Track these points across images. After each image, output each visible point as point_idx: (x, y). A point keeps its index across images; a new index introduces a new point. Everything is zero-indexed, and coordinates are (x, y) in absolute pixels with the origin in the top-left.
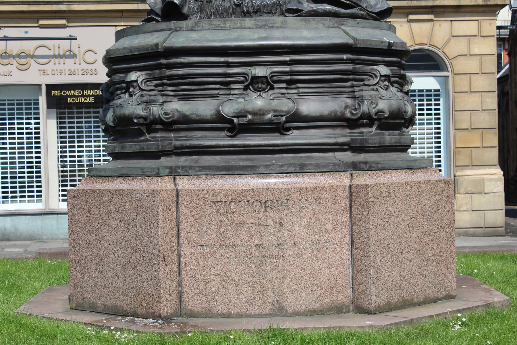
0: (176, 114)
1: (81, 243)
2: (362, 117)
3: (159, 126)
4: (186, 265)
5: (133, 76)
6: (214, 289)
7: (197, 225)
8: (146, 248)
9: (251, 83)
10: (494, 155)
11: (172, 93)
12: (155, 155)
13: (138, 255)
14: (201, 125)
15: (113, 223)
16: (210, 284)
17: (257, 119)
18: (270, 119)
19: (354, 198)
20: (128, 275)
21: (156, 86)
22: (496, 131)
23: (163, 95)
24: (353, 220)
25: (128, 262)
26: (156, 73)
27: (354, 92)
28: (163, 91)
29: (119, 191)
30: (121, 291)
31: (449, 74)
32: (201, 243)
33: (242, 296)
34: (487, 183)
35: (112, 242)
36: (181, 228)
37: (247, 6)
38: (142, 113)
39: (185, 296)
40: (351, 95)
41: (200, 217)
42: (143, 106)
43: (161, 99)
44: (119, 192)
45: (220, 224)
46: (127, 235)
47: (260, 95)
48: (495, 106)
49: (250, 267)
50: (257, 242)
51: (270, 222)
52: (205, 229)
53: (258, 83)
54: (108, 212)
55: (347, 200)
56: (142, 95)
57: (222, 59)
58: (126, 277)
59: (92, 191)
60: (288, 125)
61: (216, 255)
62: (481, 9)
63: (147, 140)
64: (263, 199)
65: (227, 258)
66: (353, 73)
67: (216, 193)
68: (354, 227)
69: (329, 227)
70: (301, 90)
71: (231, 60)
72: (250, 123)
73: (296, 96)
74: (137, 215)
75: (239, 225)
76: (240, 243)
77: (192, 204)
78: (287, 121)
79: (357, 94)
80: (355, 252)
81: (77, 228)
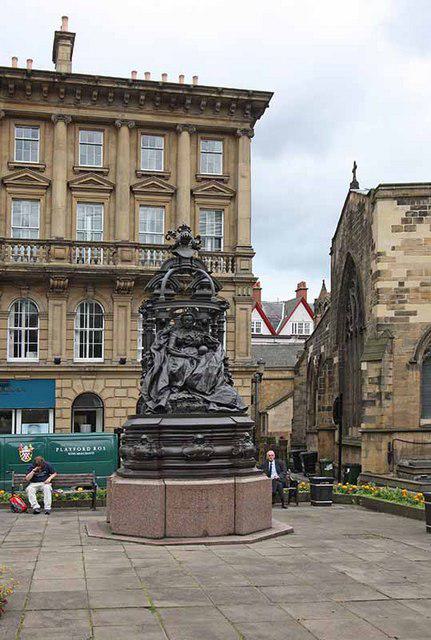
5: (144, 436)
44: (139, 486)
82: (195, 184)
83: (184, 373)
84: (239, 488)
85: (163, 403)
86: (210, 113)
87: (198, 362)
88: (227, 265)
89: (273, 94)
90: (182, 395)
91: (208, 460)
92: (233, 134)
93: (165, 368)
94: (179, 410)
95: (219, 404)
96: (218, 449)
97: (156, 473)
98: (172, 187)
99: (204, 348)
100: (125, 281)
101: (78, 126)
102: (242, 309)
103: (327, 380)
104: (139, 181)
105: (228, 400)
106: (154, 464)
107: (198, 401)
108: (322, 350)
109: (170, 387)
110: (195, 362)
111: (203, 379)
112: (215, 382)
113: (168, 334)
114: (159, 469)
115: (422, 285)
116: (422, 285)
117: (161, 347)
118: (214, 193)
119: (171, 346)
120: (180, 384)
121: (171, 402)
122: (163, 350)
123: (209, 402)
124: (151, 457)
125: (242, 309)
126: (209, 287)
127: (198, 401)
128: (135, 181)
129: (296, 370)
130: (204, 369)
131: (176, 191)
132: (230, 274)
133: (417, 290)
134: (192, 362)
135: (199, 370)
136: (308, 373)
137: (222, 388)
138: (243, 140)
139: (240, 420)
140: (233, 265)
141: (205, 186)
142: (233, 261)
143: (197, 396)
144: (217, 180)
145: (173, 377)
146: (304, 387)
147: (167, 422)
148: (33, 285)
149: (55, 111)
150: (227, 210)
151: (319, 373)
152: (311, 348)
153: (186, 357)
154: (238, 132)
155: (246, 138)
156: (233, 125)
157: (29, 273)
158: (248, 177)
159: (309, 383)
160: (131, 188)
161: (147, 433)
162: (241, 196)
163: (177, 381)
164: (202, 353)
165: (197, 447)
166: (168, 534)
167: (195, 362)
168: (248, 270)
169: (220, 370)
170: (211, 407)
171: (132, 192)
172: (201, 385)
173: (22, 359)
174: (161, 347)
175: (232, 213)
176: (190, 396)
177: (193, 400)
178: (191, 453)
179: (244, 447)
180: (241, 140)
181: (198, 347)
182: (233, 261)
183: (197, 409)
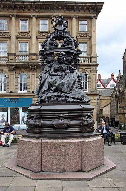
2: (84, 126)
17: (61, 126)
38: (34, 124)
45: (51, 151)
59: (23, 141)
64: (62, 145)
66: (82, 115)
67: (51, 143)
82: (78, 35)
83: (56, 83)
84: (84, 145)
85: (43, 98)
86: (82, 11)
87: (64, 77)
88: (88, 60)
90: (54, 94)
91: (66, 128)
92: (90, 18)
93: (47, 81)
94: (52, 101)
95: (74, 98)
96: (73, 122)
97: (38, 135)
99: (68, 71)
101: (39, 19)
102: (93, 74)
103: (122, 98)
105: (79, 96)
106: (37, 130)
107: (63, 97)
108: (120, 89)
109: (49, 89)
110: (62, 77)
111: (66, 86)
112: (72, 87)
113: (51, 66)
114: (41, 133)
117: (47, 72)
119: (52, 71)
120: (54, 88)
121: (48, 97)
122: (47, 73)
123: (68, 97)
124: (36, 126)
125: (93, 74)
126: (72, 45)
127: (63, 97)
129: (111, 96)
130: (66, 80)
132: (89, 63)
134: (61, 78)
135: (65, 81)
136: (115, 97)
137: (76, 90)
138: (94, 20)
139: (85, 106)
140: (90, 60)
141: (81, 35)
142: (90, 59)
143: (62, 94)
145: (50, 85)
146: (114, 101)
147: (44, 108)
148: (25, 68)
149: (33, 14)
151: (119, 96)
152: (116, 89)
153: (58, 75)
154: (92, 17)
155: (94, 19)
156: (90, 15)
157: (22, 64)
158: (95, 31)
159: (116, 100)
161: (34, 114)
162: (93, 38)
163: (53, 87)
164: (66, 74)
165: (60, 122)
166: (43, 169)
167: (62, 77)
169: (75, 81)
170: (69, 99)
172: (64, 89)
173: (23, 92)
174: (47, 72)
175: (90, 43)
176: (58, 94)
177: (60, 96)
178: (57, 125)
179: (88, 121)
180: (93, 19)
181: (64, 71)
182: (90, 59)
183: (62, 101)
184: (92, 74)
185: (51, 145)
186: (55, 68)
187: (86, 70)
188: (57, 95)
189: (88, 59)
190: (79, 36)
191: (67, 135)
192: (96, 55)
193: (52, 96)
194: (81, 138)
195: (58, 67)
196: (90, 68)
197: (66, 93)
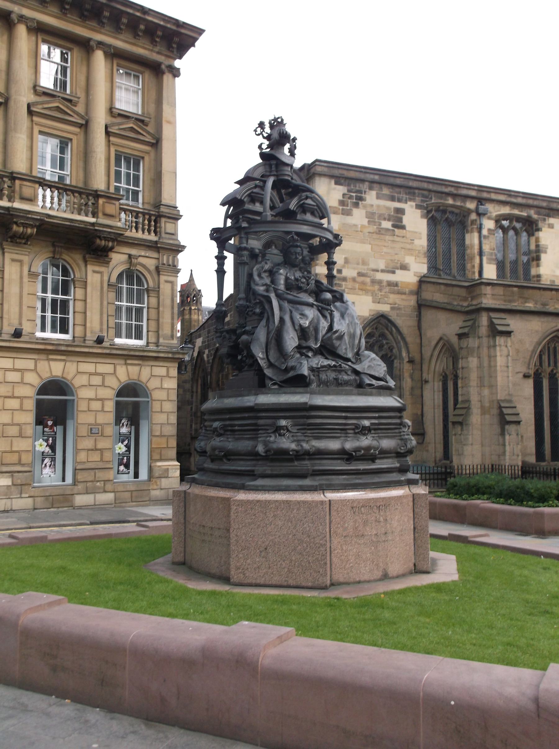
0: (314, 448)
1: (244, 537)
3: (307, 457)
4: (334, 550)
5: (283, 423)
6: (351, 565)
7: (342, 523)
8: (313, 540)
9: (361, 431)
10: (173, 453)
11: (310, 435)
12: (303, 476)
13: (305, 545)
14: (330, 456)
15: (280, 523)
16: (349, 562)
18: (372, 453)
19: (416, 501)
20: (293, 558)
21: (298, 430)
22: (176, 437)
23: (306, 436)
24: (415, 516)
25: (295, 549)
26: (302, 421)
27: (401, 436)
28: (306, 433)
29: (287, 501)
30: (286, 570)
31: (149, 400)
32: (344, 535)
33: (367, 568)
34: (170, 471)
35: (277, 536)
36: (332, 525)
37: (341, 380)
39: (333, 571)
40: (399, 438)
41: (344, 518)
42: (295, 443)
43: (307, 439)
44: (287, 502)
45: (355, 522)
46: (294, 531)
47: (367, 438)
48: (175, 421)
49: (371, 549)
50: (375, 532)
51: (382, 519)
52: (346, 525)
53: (365, 430)
54: (275, 516)
55: (412, 503)
56: (292, 436)
57: (344, 414)
58: (291, 560)
60: (379, 456)
61: (353, 542)
62: (170, 360)
63: (296, 466)
64: (378, 504)
65: (359, 544)
67: (353, 501)
68: (416, 520)
69: (406, 520)
70: (380, 435)
71: (349, 415)
72: (362, 455)
73: (377, 438)
74: (305, 518)
75: (365, 523)
76: (366, 533)
77: (339, 509)
78: (378, 454)
79: (402, 437)
80: (416, 535)
81: (241, 527)
82: (110, 120)
86: (128, 36)
89: (203, 31)
98: (82, 117)
100: (25, 226)
102: (167, 282)
104: (38, 99)
115: (360, 274)
116: (360, 274)
118: (132, 135)
125: (167, 282)
128: (32, 98)
131: (87, 122)
132: (153, 237)
133: (354, 280)
138: (167, 77)
140: (155, 227)
144: (137, 119)
150: (147, 158)
155: (170, 76)
158: (172, 123)
160: (29, 106)
161: (285, 418)
162: (165, 145)
165: (366, 441)
168: (174, 234)
171: (30, 113)
178: (357, 450)
182: (155, 221)
184: (163, 278)
185: (354, 505)
186: (287, 279)
187: (141, 260)
188: (335, 366)
189: (150, 221)
190: (113, 124)
191: (376, 479)
192: (175, 212)
193: (323, 367)
194: (407, 486)
195: (297, 280)
196: (155, 255)
197: (348, 360)
